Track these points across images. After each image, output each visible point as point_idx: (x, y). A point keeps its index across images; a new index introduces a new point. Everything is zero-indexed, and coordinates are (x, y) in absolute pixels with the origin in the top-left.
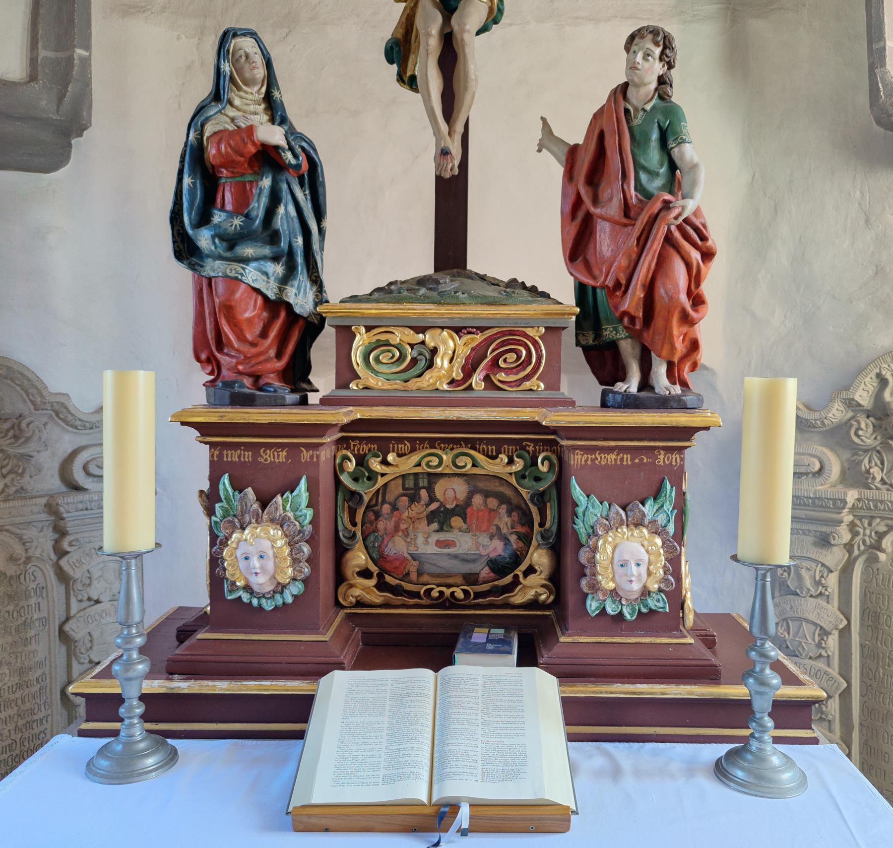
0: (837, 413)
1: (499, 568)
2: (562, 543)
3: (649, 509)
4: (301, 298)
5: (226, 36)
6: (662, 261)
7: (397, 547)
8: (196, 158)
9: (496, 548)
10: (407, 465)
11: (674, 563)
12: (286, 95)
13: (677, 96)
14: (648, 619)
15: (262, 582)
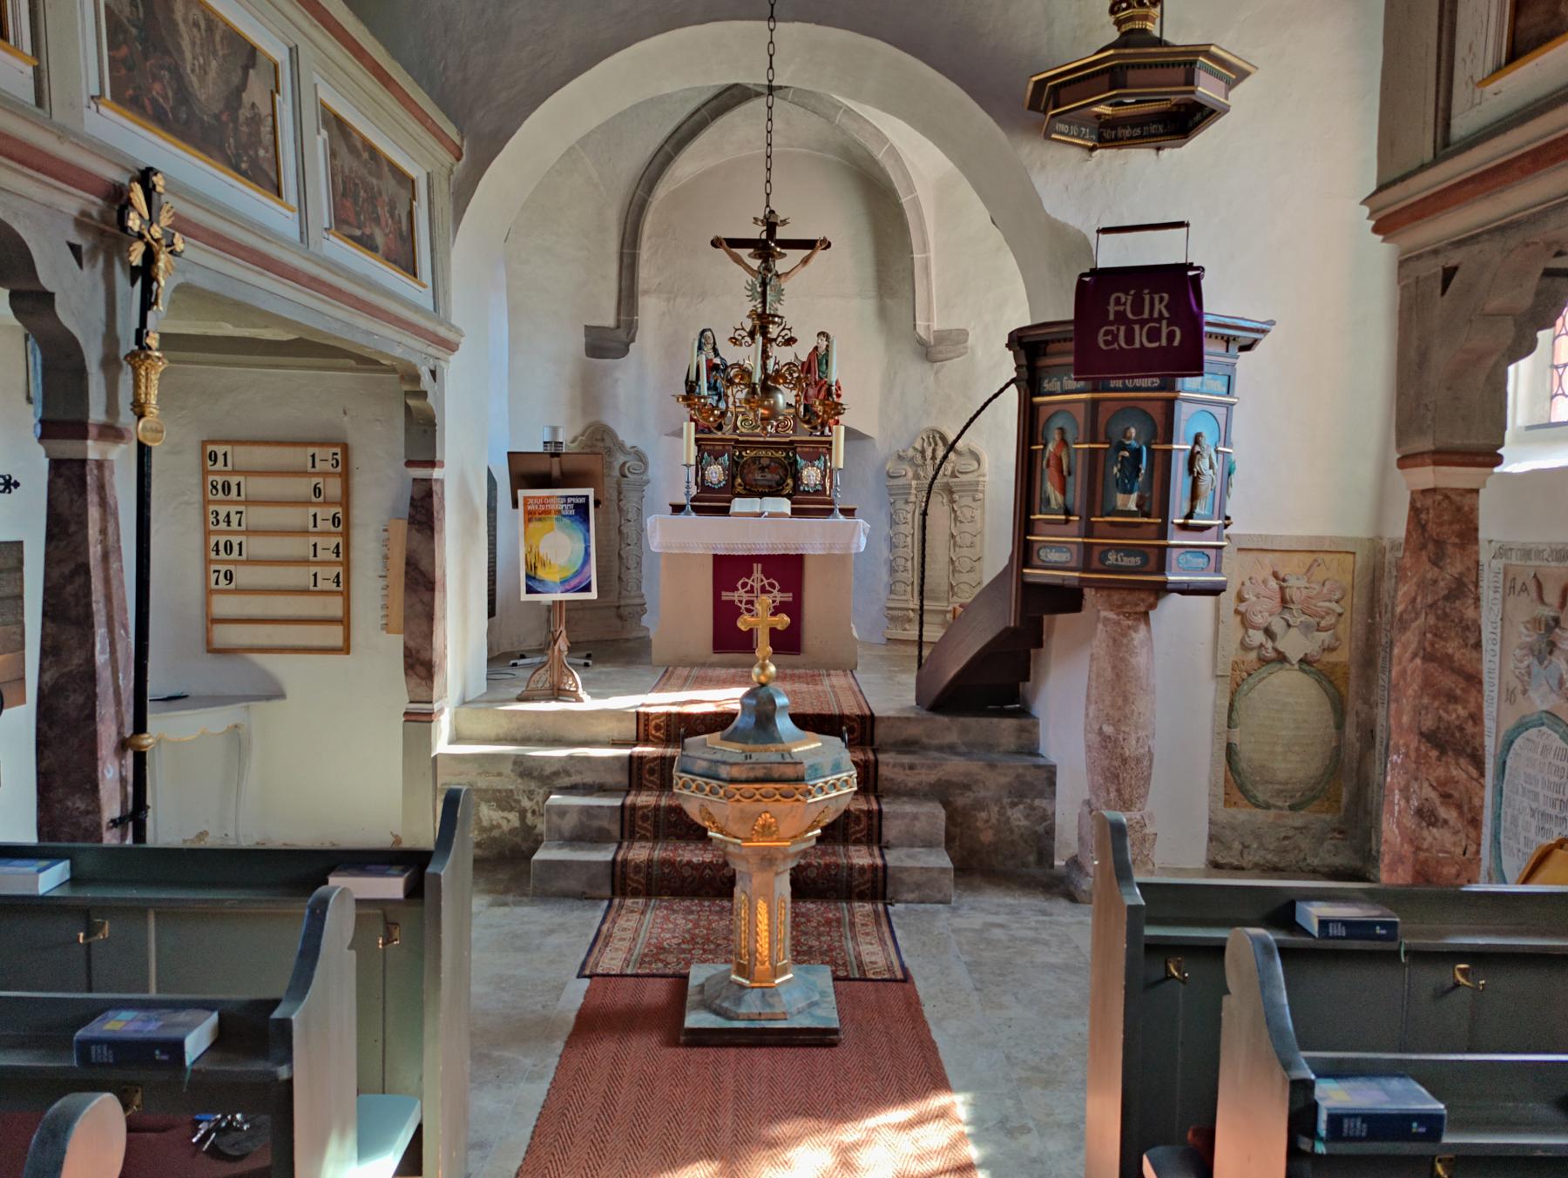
0: (911, 452)
11: (824, 477)
12: (718, 346)
14: (816, 492)
15: (715, 480)
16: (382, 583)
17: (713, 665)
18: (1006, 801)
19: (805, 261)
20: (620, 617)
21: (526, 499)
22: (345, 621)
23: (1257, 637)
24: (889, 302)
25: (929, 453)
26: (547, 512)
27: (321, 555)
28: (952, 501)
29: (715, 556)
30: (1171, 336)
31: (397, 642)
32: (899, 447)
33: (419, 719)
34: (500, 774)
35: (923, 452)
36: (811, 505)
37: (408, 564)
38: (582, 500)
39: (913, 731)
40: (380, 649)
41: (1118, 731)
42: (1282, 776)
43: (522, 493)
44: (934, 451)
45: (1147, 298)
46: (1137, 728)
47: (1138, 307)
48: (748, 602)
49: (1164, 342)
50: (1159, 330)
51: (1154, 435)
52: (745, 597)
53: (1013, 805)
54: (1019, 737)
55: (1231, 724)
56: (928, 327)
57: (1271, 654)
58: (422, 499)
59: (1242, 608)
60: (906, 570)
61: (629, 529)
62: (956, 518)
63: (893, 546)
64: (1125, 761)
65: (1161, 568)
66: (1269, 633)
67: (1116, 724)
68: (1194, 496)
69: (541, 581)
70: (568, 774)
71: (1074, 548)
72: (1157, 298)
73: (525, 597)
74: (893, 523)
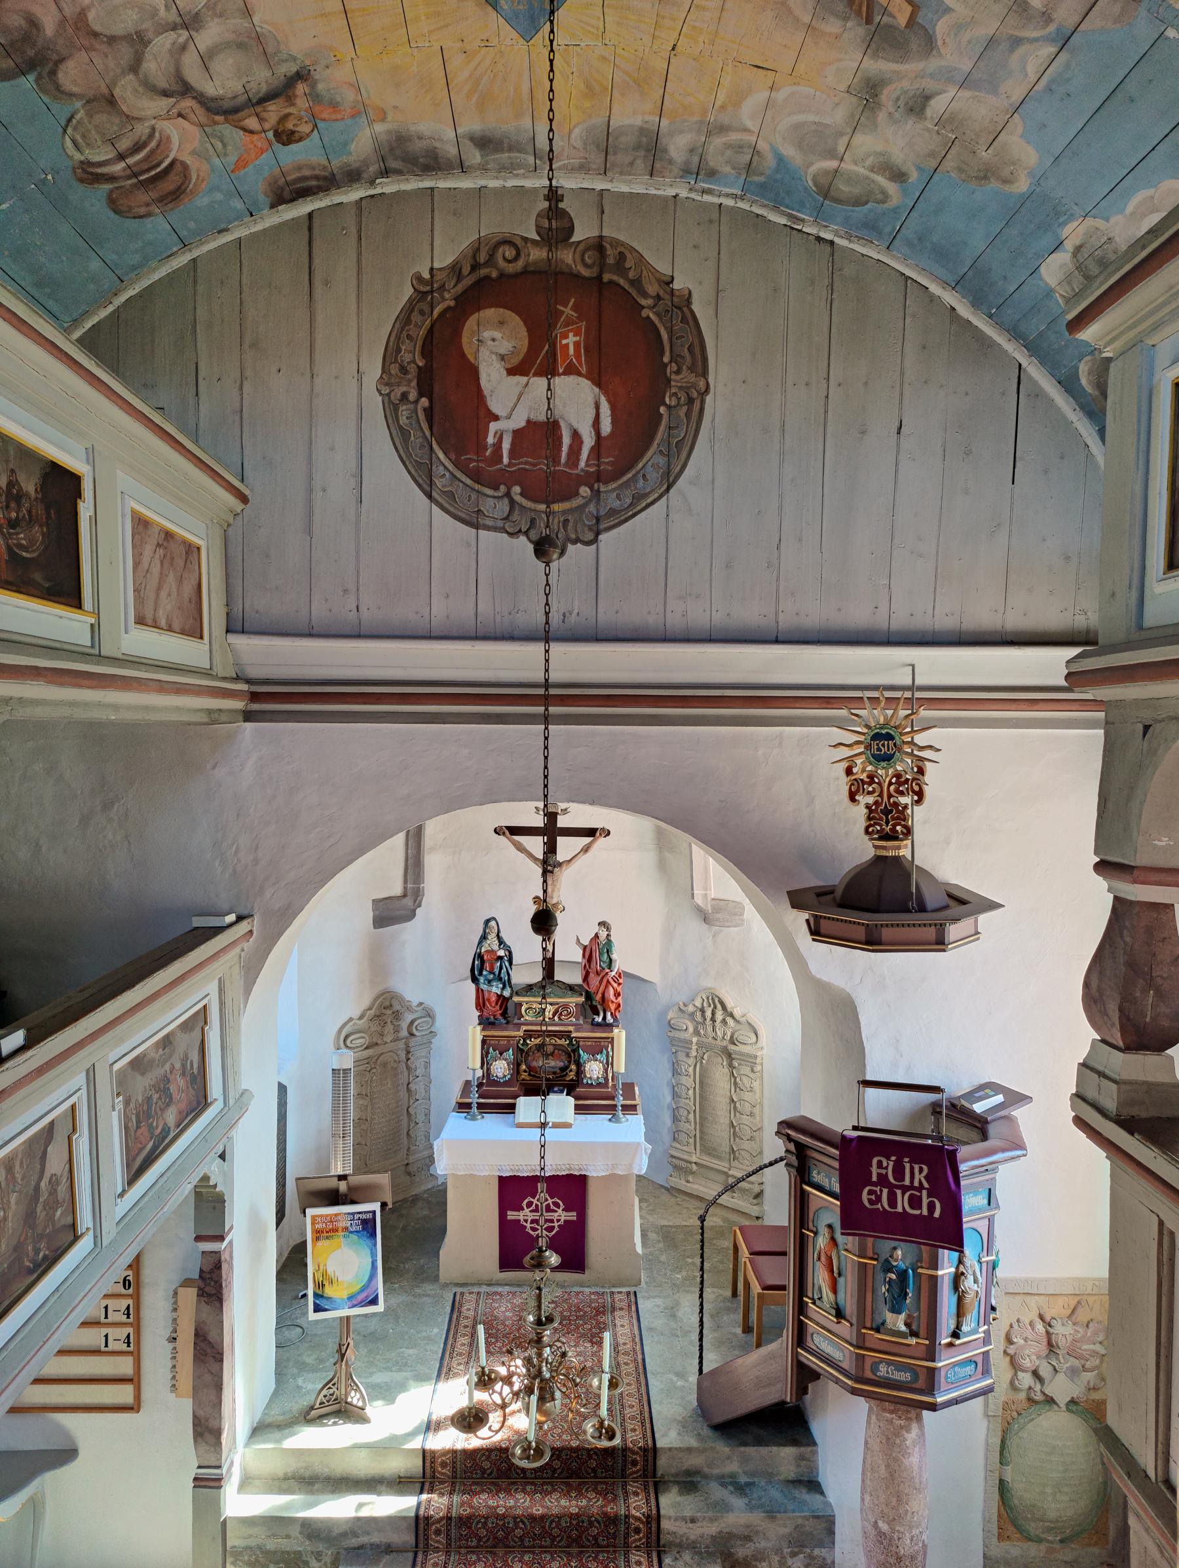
0: (691, 1009)
1: (564, 1069)
2: (579, 1065)
3: (599, 1057)
4: (507, 993)
5: (487, 922)
6: (606, 987)
7: (534, 1064)
8: (479, 956)
9: (562, 1064)
10: (538, 1041)
11: (606, 1071)
13: (612, 938)
14: (599, 1085)
15: (500, 1075)
16: (171, 1346)
17: (498, 1284)
18: (786, 1551)
19: (586, 849)
20: (409, 1174)
21: (313, 1217)
22: (133, 1380)
23: (1026, 1380)
24: (667, 855)
25: (708, 1014)
26: (335, 1230)
27: (112, 1317)
28: (731, 1066)
29: (500, 1178)
30: (931, 1207)
31: (186, 1406)
32: (680, 998)
33: (208, 1483)
34: (288, 1537)
35: (703, 1011)
36: (596, 1100)
37: (197, 1335)
38: (370, 1216)
39: (695, 1461)
40: (169, 1410)
41: (893, 1530)
42: (1052, 1515)
43: (310, 1212)
44: (713, 1014)
45: (907, 1166)
46: (911, 1528)
47: (899, 1172)
48: (533, 1221)
49: (925, 1212)
50: (920, 1198)
51: (920, 1260)
52: (531, 1216)
53: (794, 1555)
54: (798, 1466)
55: (1003, 1461)
56: (706, 895)
57: (1039, 1397)
58: (211, 1272)
59: (1011, 1351)
60: (688, 1121)
61: (418, 1086)
62: (735, 1133)
63: (675, 1095)
64: (899, 1559)
65: (930, 1389)
66: (1035, 1374)
67: (891, 1522)
68: (960, 1313)
69: (329, 1298)
70: (355, 1535)
71: (846, 1352)
72: (916, 1167)
73: (313, 1316)
74: (675, 1072)
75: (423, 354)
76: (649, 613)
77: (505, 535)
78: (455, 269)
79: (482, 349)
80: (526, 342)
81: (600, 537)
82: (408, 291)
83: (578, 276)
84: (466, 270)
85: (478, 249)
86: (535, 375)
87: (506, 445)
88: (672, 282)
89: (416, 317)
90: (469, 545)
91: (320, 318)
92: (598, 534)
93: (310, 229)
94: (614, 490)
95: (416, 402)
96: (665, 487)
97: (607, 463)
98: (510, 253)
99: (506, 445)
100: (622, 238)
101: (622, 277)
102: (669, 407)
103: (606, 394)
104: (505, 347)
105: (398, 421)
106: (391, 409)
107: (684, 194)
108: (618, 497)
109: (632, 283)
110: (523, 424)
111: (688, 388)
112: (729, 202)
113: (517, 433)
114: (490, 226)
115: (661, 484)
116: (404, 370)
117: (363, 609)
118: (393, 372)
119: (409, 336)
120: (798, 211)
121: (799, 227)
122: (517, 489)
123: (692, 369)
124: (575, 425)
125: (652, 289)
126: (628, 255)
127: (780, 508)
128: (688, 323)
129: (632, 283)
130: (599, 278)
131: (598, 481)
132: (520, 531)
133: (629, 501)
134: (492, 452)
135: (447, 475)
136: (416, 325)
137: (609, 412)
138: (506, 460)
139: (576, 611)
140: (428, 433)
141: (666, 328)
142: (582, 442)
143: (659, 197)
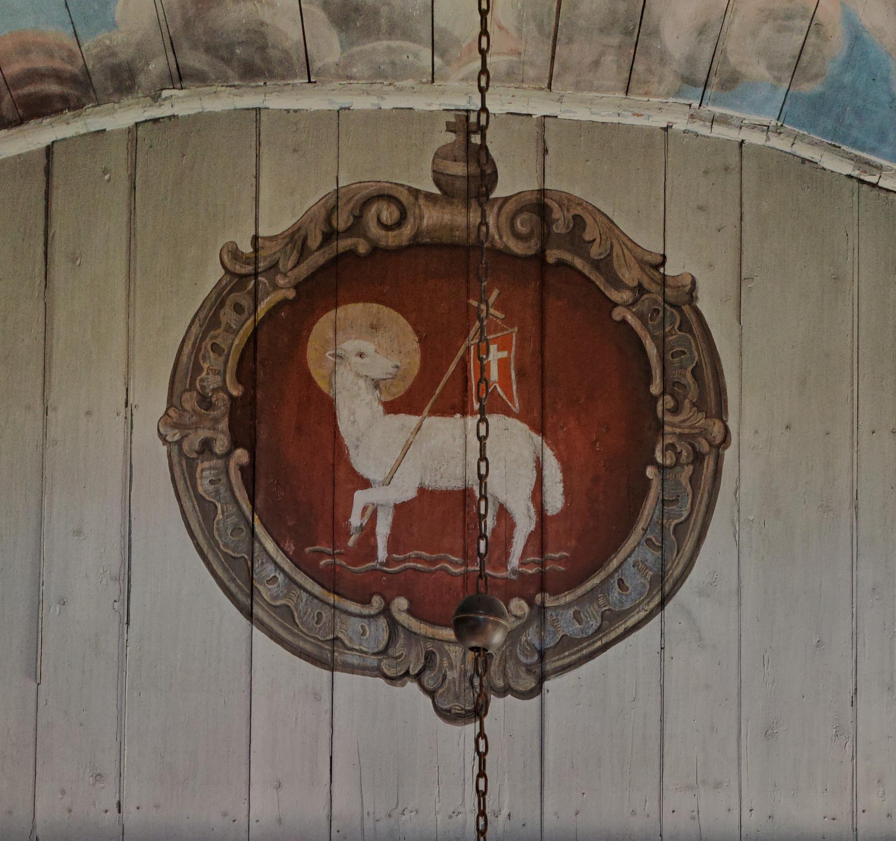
75: (239, 377)
76: (634, 813)
77: (381, 681)
78: (296, 240)
79: (341, 370)
80: (417, 359)
81: (547, 684)
82: (214, 274)
83: (505, 255)
84: (314, 241)
85: (336, 207)
86: (433, 412)
87: (383, 530)
88: (663, 264)
89: (228, 316)
90: (317, 697)
91: (60, 316)
92: (542, 678)
93: (48, 171)
94: (568, 605)
95: (228, 455)
96: (657, 600)
97: (559, 561)
98: (389, 214)
99: (383, 530)
100: (577, 192)
101: (580, 256)
102: (662, 468)
103: (554, 446)
104: (382, 365)
105: (194, 487)
106: (183, 468)
107: (681, 124)
108: (577, 617)
109: (596, 265)
110: (411, 494)
111: (694, 436)
112: (755, 138)
113: (400, 508)
114: (356, 171)
115: (650, 596)
116: (206, 402)
117: (128, 807)
118: (187, 406)
119: (215, 347)
120: (873, 151)
121: (873, 179)
122: (401, 603)
123: (700, 405)
124: (503, 498)
125: (630, 275)
126: (589, 220)
127: (855, 635)
128: (691, 331)
129: (596, 265)
130: (540, 257)
131: (542, 590)
132: (407, 673)
133: (595, 624)
134: (359, 543)
135: (281, 577)
136: (228, 329)
137: (560, 476)
138: (382, 554)
139: (505, 812)
140: (246, 507)
141: (654, 338)
142: (513, 526)
143: (641, 129)
